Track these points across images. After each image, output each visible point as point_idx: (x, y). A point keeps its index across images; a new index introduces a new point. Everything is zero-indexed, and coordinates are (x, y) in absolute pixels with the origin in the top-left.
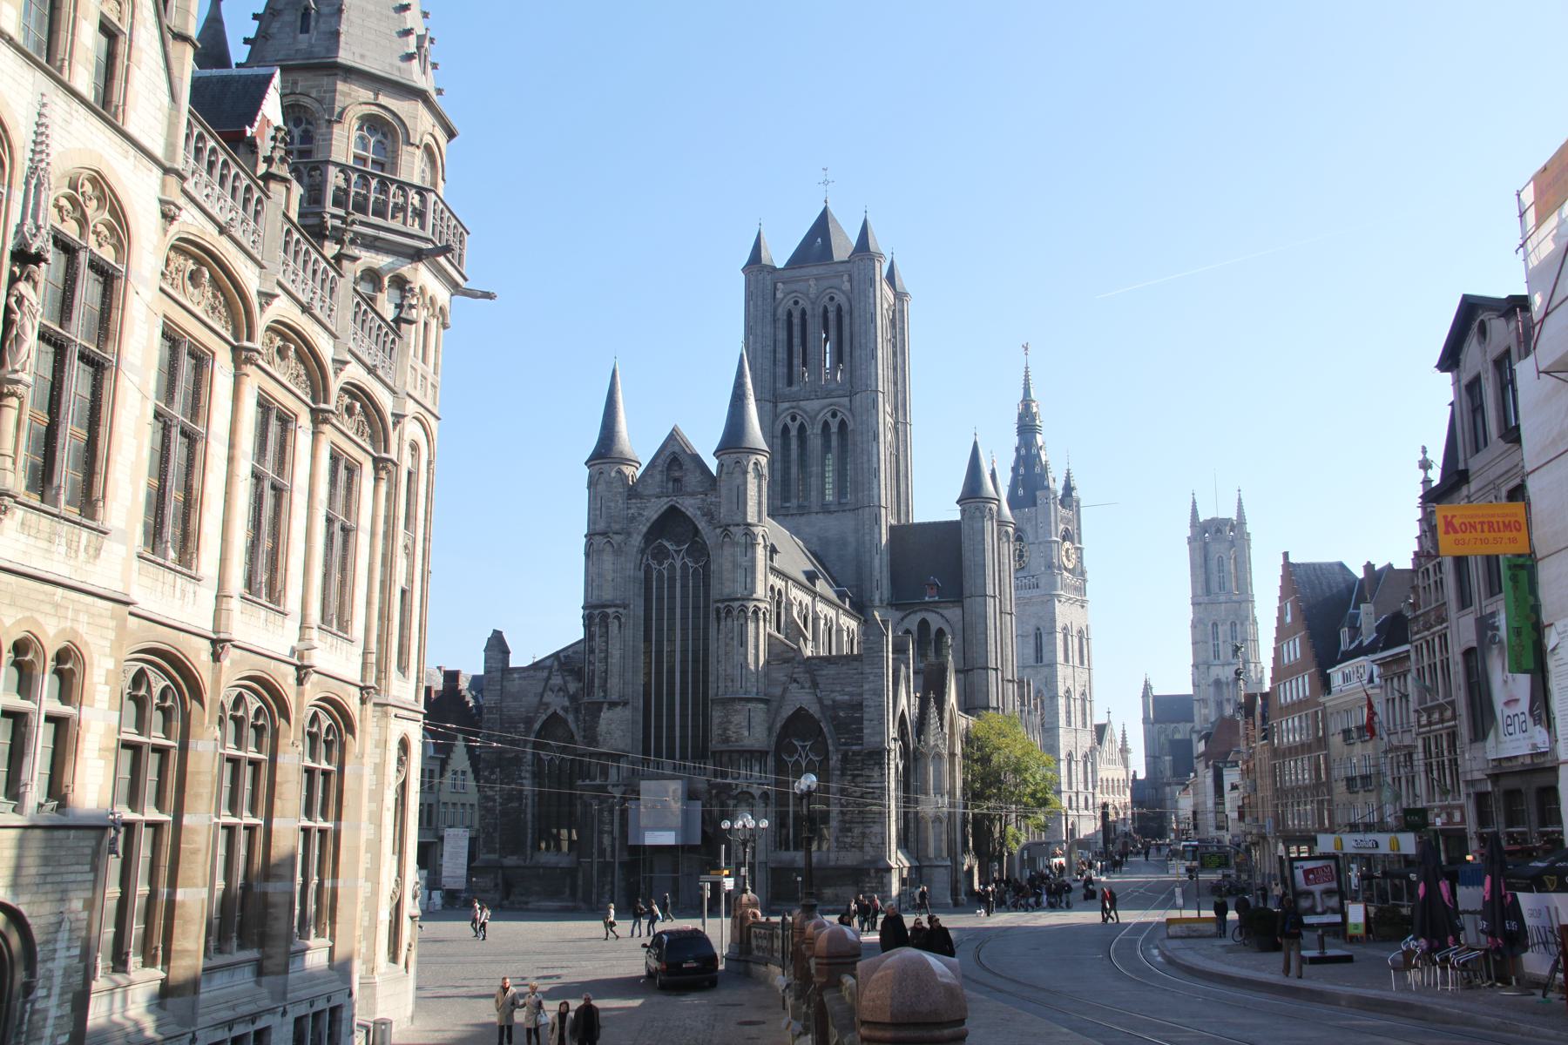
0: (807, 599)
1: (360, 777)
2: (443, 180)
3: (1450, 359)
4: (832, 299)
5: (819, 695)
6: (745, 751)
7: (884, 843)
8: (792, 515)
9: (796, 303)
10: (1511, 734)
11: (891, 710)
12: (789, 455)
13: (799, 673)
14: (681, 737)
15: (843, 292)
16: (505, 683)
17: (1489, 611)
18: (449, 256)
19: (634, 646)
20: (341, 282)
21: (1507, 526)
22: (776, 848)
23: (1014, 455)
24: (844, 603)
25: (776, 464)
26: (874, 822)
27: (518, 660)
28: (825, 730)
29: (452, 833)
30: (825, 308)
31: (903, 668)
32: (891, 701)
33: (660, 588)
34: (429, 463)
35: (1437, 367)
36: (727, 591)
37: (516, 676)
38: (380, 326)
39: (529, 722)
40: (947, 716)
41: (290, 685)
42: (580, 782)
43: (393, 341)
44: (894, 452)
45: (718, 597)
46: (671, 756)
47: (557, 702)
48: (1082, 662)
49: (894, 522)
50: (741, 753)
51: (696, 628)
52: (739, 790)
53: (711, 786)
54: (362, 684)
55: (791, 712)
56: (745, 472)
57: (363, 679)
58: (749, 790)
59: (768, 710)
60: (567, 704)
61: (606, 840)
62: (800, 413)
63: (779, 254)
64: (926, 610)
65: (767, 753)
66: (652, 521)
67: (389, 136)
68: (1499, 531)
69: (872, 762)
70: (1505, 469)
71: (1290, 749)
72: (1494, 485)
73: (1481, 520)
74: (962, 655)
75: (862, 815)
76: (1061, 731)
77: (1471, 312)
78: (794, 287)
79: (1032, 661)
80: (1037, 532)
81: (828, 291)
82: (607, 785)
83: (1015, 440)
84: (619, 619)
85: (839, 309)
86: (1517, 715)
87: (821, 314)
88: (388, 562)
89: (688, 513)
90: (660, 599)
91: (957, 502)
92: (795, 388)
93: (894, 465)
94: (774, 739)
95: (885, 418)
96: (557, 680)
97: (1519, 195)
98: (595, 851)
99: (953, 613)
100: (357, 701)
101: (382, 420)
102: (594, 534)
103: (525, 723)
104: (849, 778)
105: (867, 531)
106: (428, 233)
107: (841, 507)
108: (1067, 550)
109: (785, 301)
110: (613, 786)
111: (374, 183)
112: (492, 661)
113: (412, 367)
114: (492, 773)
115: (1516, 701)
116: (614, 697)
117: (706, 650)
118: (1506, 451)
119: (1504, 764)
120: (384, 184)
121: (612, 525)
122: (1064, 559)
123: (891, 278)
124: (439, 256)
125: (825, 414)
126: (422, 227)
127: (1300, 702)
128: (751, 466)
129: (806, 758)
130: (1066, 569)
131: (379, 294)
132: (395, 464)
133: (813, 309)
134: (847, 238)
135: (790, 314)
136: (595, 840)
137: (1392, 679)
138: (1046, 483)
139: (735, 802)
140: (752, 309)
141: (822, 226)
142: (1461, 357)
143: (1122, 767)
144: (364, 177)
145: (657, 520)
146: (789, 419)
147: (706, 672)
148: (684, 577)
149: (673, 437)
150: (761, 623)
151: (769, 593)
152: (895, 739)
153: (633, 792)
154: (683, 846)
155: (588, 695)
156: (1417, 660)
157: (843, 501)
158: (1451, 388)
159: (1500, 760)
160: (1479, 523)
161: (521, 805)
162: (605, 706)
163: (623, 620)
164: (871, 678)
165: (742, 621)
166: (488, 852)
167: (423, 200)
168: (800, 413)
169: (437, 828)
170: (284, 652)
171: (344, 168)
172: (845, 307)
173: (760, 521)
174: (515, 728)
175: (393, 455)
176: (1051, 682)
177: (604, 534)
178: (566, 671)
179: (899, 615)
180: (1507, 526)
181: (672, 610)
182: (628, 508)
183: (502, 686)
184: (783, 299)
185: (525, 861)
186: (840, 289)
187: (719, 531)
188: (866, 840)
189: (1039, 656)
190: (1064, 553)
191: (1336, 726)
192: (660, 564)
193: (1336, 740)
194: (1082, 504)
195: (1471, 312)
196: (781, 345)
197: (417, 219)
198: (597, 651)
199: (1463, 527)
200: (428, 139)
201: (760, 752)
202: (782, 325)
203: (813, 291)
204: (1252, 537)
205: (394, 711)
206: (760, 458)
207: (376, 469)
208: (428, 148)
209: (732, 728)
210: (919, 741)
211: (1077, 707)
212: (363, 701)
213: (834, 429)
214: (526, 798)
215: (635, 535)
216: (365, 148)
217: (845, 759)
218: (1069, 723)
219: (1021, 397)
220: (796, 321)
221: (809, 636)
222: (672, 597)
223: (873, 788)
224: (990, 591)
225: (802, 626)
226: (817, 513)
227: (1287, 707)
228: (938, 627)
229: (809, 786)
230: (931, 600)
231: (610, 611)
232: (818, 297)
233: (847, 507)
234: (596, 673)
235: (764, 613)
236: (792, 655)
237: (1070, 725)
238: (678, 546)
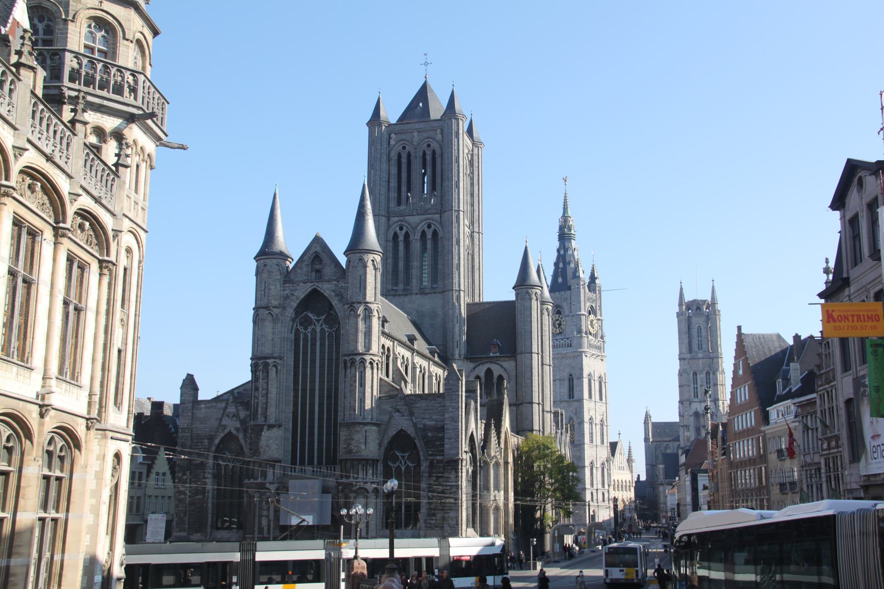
0: (407, 354)
1: (84, 482)
2: (150, 65)
3: (838, 202)
4: (429, 146)
5: (414, 421)
6: (362, 460)
7: (457, 524)
8: (399, 295)
9: (404, 148)
10: (875, 458)
11: (464, 432)
12: (398, 254)
13: (400, 405)
14: (318, 449)
15: (437, 141)
16: (194, 411)
17: (861, 373)
18: (155, 119)
19: (286, 386)
20: (75, 140)
21: (870, 318)
22: (383, 527)
23: (556, 254)
24: (434, 357)
25: (388, 260)
26: (451, 510)
27: (205, 394)
28: (418, 445)
29: (153, 518)
30: (424, 154)
31: (473, 403)
32: (464, 426)
33: (305, 346)
34: (140, 262)
35: (829, 207)
36: (352, 348)
37: (202, 406)
38: (103, 169)
39: (211, 438)
40: (503, 436)
41: (34, 418)
42: (246, 481)
43: (113, 180)
44: (471, 252)
45: (347, 353)
46: (311, 463)
47: (232, 425)
48: (601, 399)
49: (469, 301)
50: (360, 461)
51: (330, 373)
52: (358, 487)
53: (339, 484)
54: (87, 417)
55: (394, 433)
56: (365, 267)
57: (89, 412)
58: (365, 487)
59: (379, 431)
60: (239, 426)
61: (264, 522)
62: (406, 224)
63: (392, 114)
64: (491, 362)
65: (378, 461)
67: (110, 33)
68: (865, 321)
69: (450, 468)
70: (872, 278)
71: (741, 462)
72: (865, 289)
73: (853, 313)
74: (515, 394)
75: (442, 504)
76: (586, 447)
77: (853, 169)
78: (403, 137)
79: (566, 397)
80: (571, 308)
81: (426, 140)
82: (266, 483)
83: (556, 244)
84: (275, 366)
85: (434, 153)
86: (879, 445)
87: (421, 155)
88: (108, 330)
89: (326, 294)
90: (305, 353)
91: (513, 288)
92: (402, 207)
93: (470, 261)
94: (383, 451)
95: (464, 230)
96: (232, 409)
97: (881, 95)
98: (256, 529)
99: (509, 365)
100: (84, 428)
101: (105, 233)
102: (260, 308)
103: (208, 439)
104: (434, 478)
105: (450, 307)
106: (139, 103)
107: (433, 291)
108: (592, 321)
109: (396, 146)
110: (270, 483)
111: (100, 66)
112: (186, 395)
113: (127, 196)
114: (184, 474)
115: (879, 436)
116: (272, 421)
117: (337, 389)
118: (874, 266)
119: (872, 479)
120: (106, 67)
121: (273, 301)
122: (590, 327)
123: (470, 132)
124: (147, 120)
125: (423, 226)
126: (135, 99)
127: (748, 430)
128: (370, 264)
129: (405, 464)
130: (590, 334)
131: (103, 145)
132: (114, 264)
133: (415, 152)
134: (440, 103)
135: (399, 156)
136: (257, 521)
137: (807, 416)
138: (577, 274)
139: (355, 495)
140: (373, 152)
141: (423, 94)
142: (846, 200)
143: (628, 472)
144: (92, 62)
145: (303, 299)
146: (398, 229)
147: (336, 404)
148: (322, 338)
149: (317, 240)
150: (375, 370)
151: (381, 350)
152: (466, 452)
153: (283, 488)
154: (318, 526)
155: (254, 420)
156: (821, 404)
157: (434, 286)
158: (839, 221)
159: (869, 476)
160: (851, 315)
161: (204, 497)
162: (265, 428)
163: (279, 367)
164: (450, 409)
165: (362, 369)
166: (180, 531)
167: (136, 82)
168: (406, 224)
169: (143, 515)
170: (32, 396)
171: (77, 55)
172: (438, 152)
173: (375, 301)
175: (113, 258)
176: (579, 412)
177: (267, 308)
178: (239, 403)
179: (472, 365)
180: (870, 318)
181: (313, 361)
182: (284, 290)
183: (193, 413)
184: (395, 145)
185: (206, 537)
186: (434, 139)
187: (347, 306)
188: (445, 522)
189: (571, 394)
190: (589, 323)
191: (772, 447)
192: (306, 329)
193: (773, 457)
194: (602, 289)
195: (853, 169)
196: (393, 177)
197: (132, 94)
198: (260, 389)
199: (840, 318)
200: (139, 36)
201: (373, 460)
202: (394, 162)
203: (416, 140)
204: (721, 313)
205: (111, 434)
206: (376, 256)
207: (101, 268)
208: (139, 42)
209: (354, 443)
210: (483, 453)
211: (597, 430)
212: (88, 428)
213: (429, 236)
214: (208, 492)
215: (288, 309)
216: (94, 42)
217: (431, 465)
218: (592, 441)
219: (561, 214)
220: (404, 160)
221: (409, 379)
222: (313, 352)
223: (450, 486)
224: (535, 349)
225: (404, 373)
226: (416, 294)
227: (739, 433)
228: (499, 374)
229: (392, 488)
230: (494, 355)
231: (270, 361)
232: (419, 144)
233: (438, 290)
234: (260, 404)
235: (377, 364)
236: (396, 393)
237: (592, 442)
238: (318, 317)
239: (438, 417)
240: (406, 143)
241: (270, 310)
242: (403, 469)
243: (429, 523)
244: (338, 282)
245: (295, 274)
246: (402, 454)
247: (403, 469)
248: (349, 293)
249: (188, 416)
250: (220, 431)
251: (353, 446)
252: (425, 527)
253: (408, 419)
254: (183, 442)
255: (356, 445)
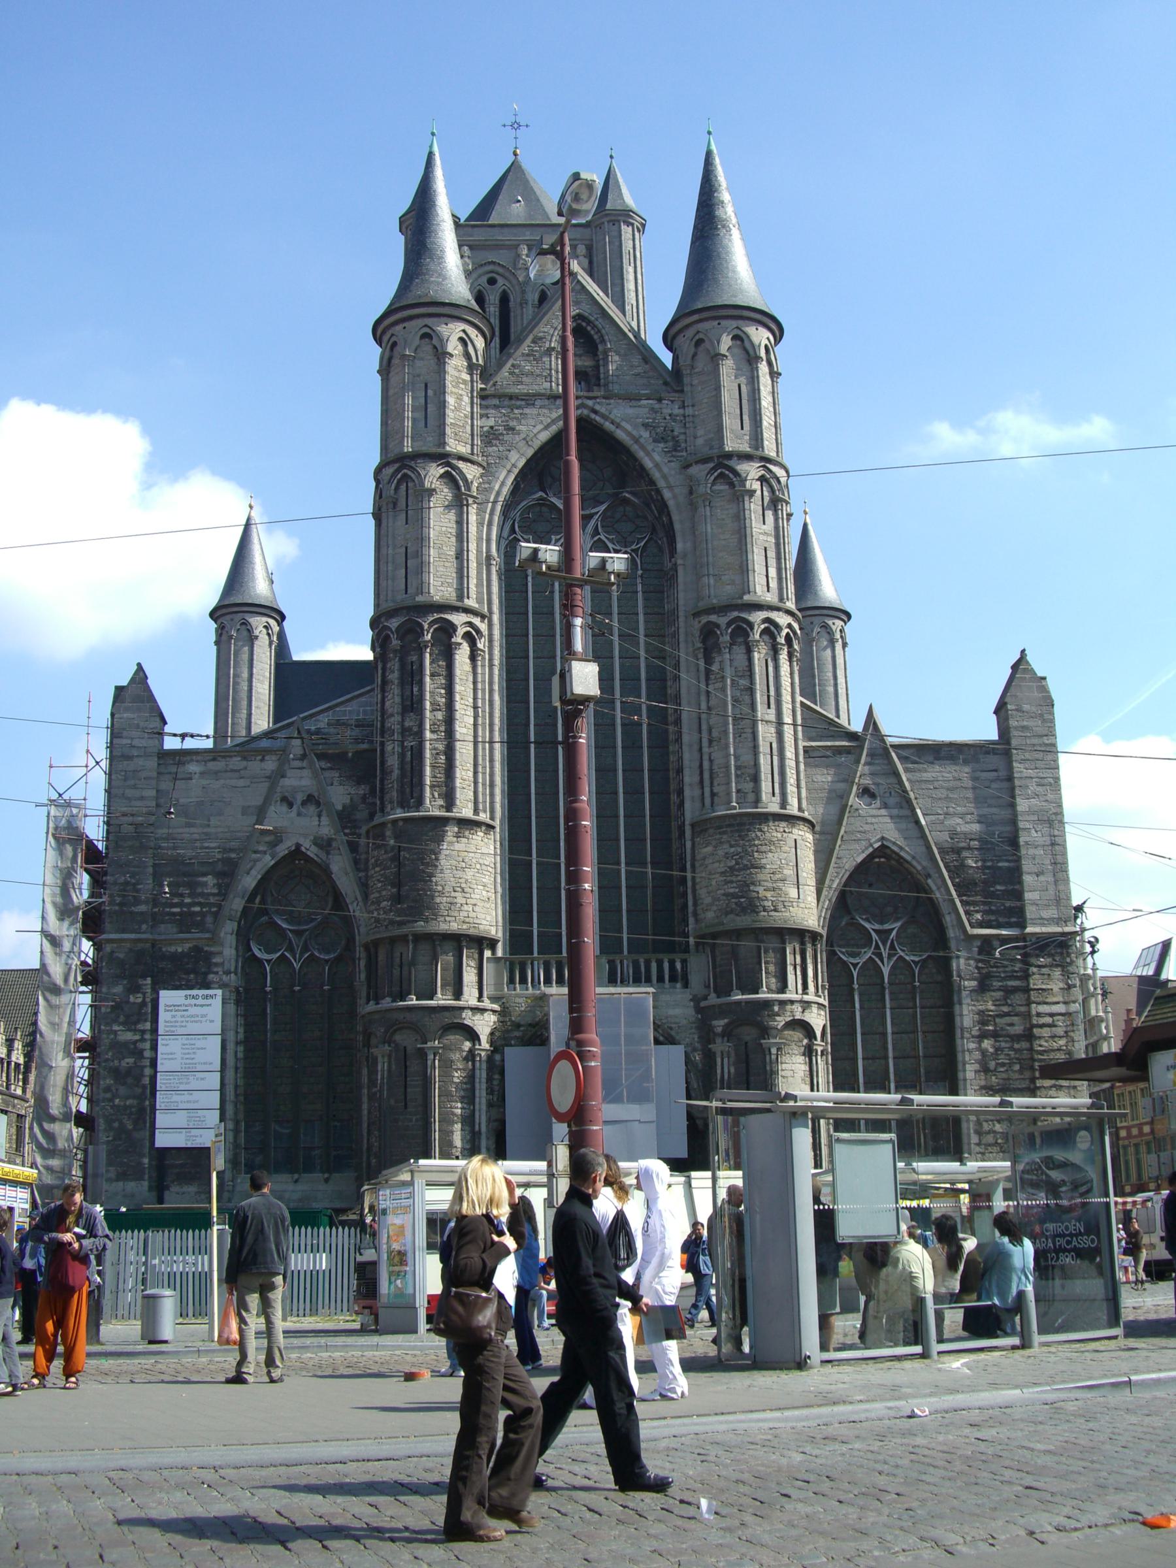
9: (492, 282)
37: (193, 768)
39: (227, 872)
66: (537, 444)
89: (620, 435)
96: (299, 780)
104: (999, 994)
112: (134, 733)
116: (467, 812)
129: (890, 956)
155: (403, 807)
162: (452, 830)
164: (1033, 787)
174: (192, 885)
187: (698, 471)
223: (1052, 1015)
231: (458, 619)
239: (994, 810)
240: (500, 270)
241: (449, 464)
242: (886, 971)
243: (989, 1132)
244: (660, 400)
245: (511, 373)
246: (877, 927)
247: (886, 971)
248: (700, 433)
249: (142, 798)
250: (261, 848)
251: (760, 889)
252: (978, 1144)
253: (907, 817)
254: (127, 883)
255: (769, 885)
